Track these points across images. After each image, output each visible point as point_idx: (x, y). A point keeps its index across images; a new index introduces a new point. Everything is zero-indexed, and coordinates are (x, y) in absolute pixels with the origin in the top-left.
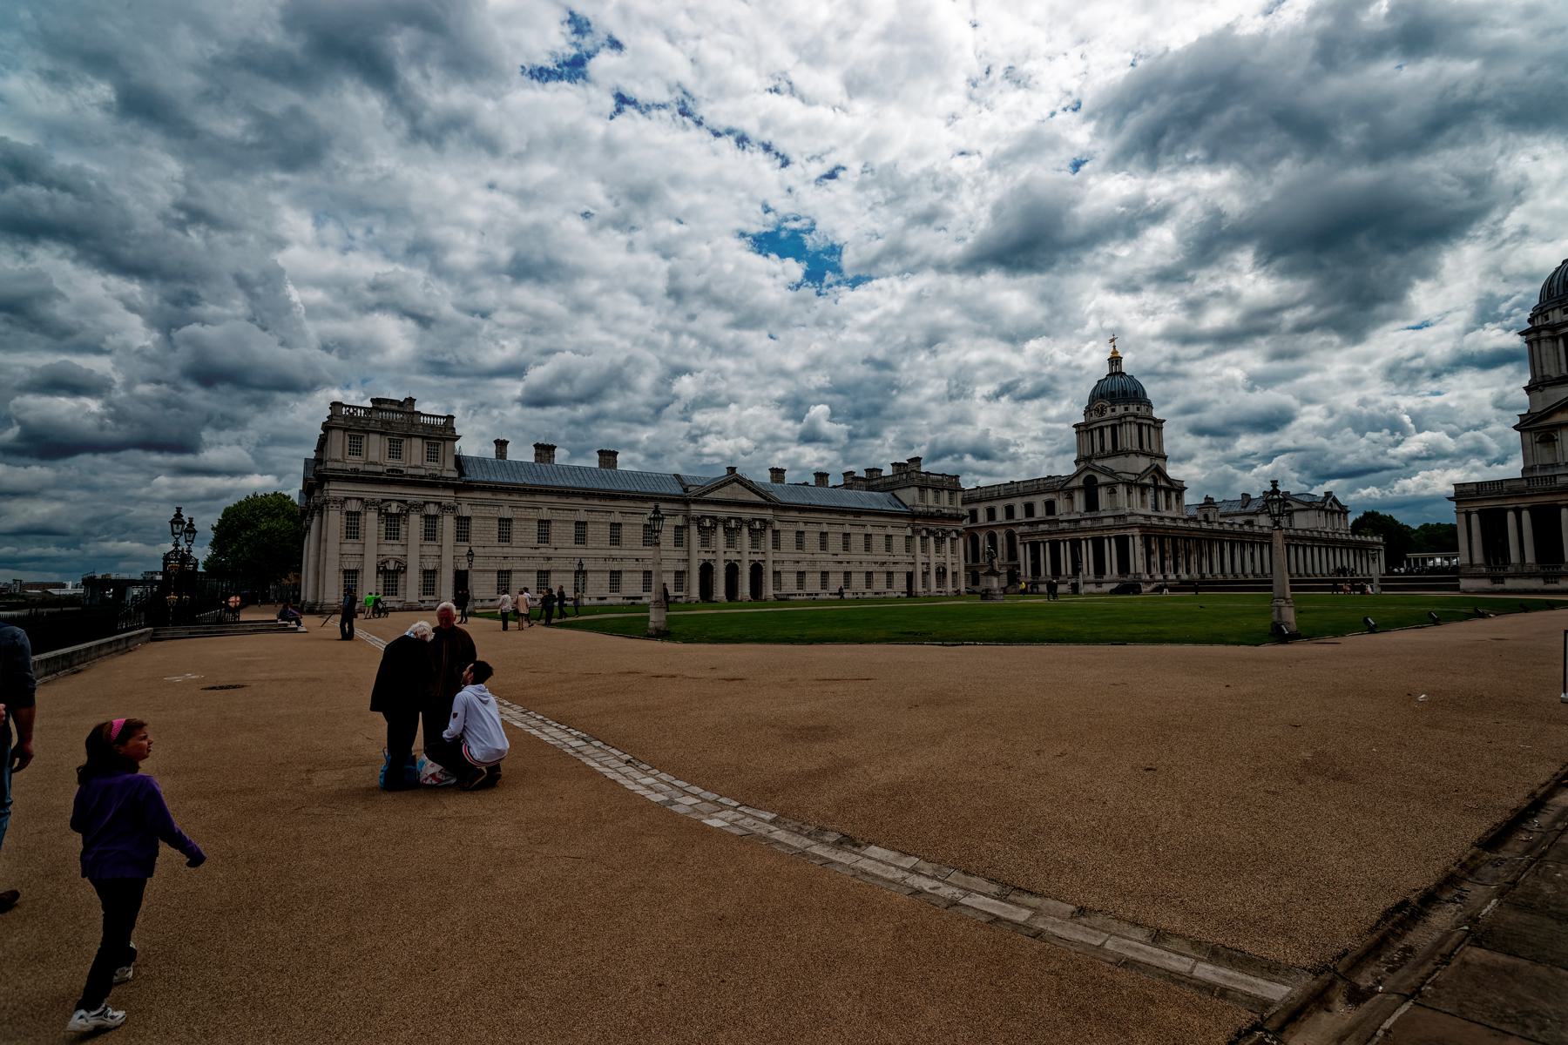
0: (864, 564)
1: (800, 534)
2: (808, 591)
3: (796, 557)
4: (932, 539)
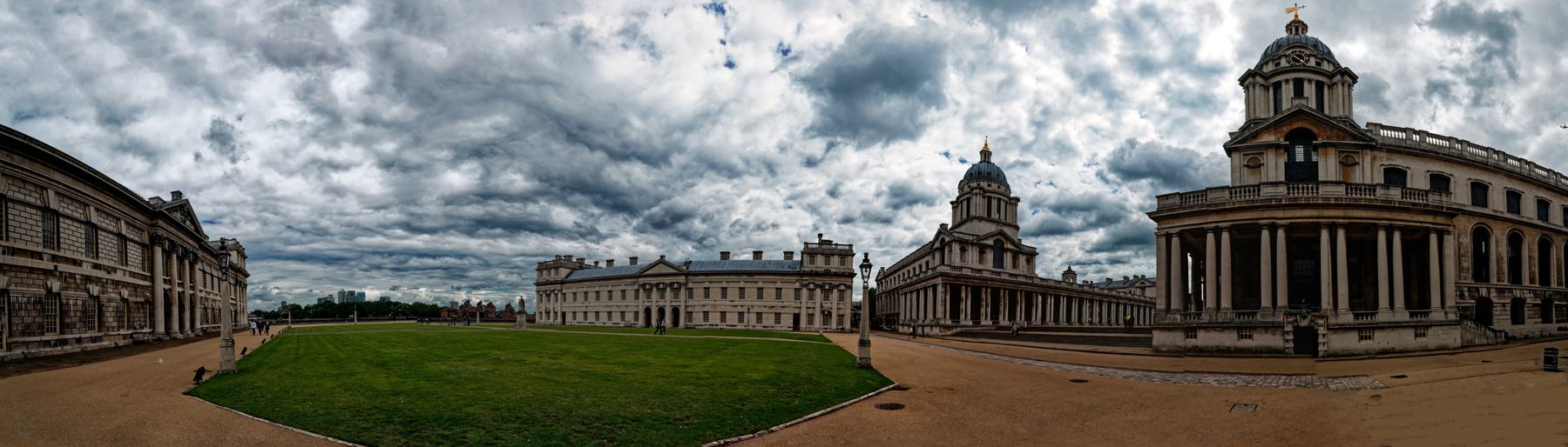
0: (756, 308)
1: (707, 289)
2: (710, 322)
3: (703, 303)
4: (818, 290)
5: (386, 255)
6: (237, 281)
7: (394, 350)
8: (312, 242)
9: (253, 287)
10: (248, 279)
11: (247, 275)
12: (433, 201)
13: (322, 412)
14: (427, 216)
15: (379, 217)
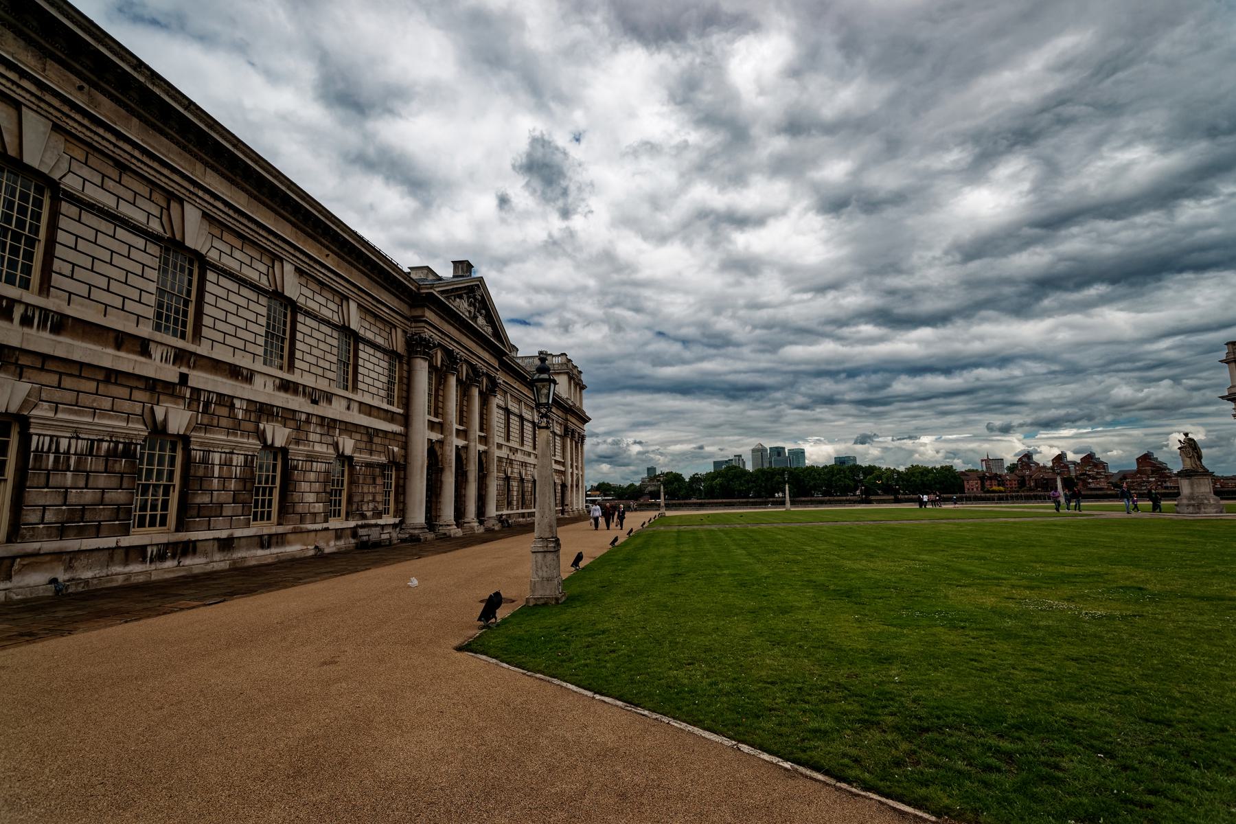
5: (843, 376)
6: (566, 429)
7: (872, 565)
8: (701, 359)
9: (595, 440)
10: (587, 427)
11: (584, 420)
12: (934, 258)
13: (727, 686)
14: (925, 289)
15: (825, 305)
